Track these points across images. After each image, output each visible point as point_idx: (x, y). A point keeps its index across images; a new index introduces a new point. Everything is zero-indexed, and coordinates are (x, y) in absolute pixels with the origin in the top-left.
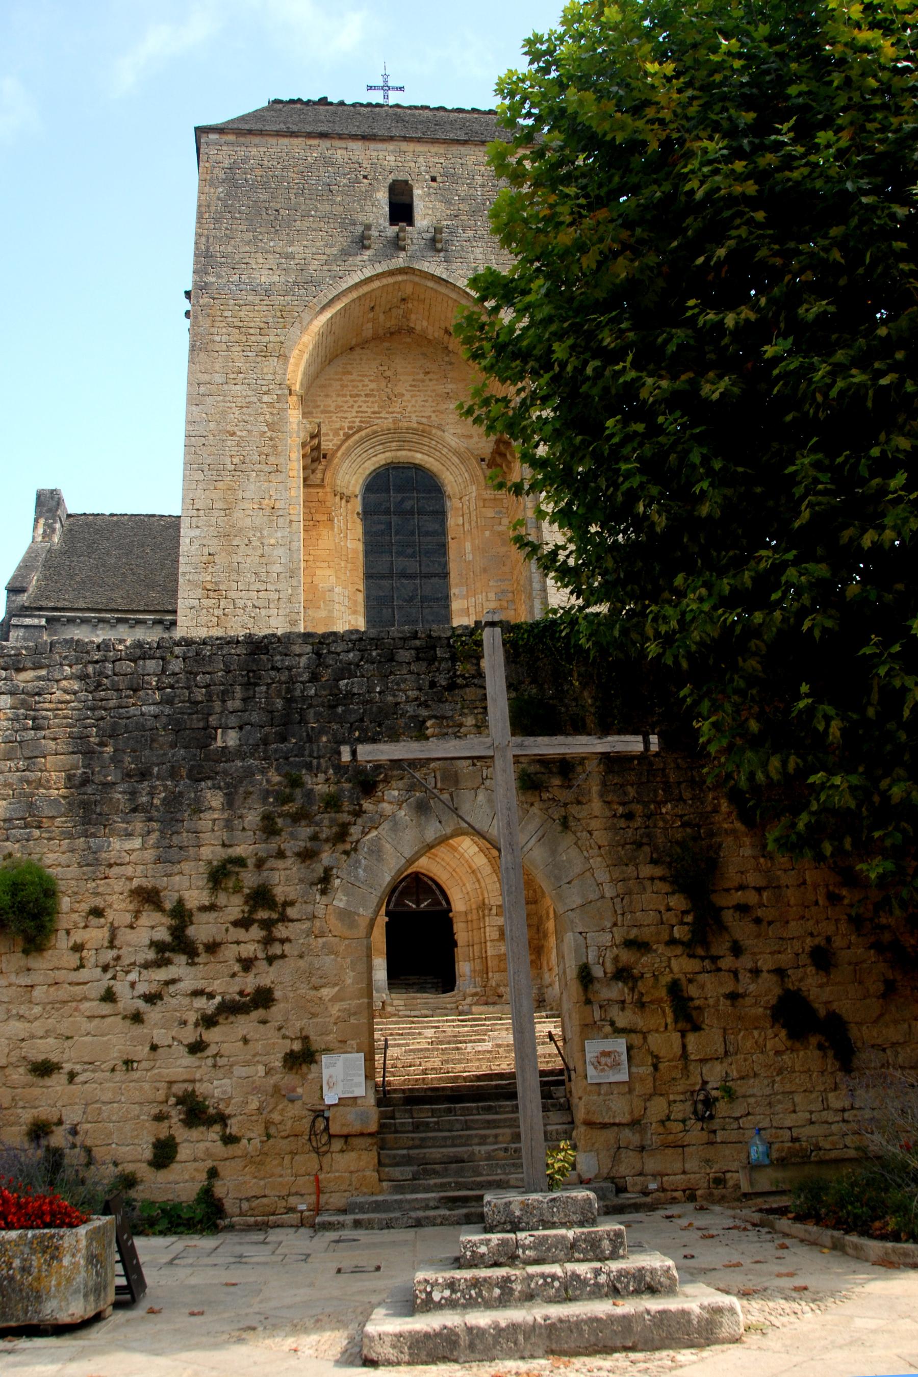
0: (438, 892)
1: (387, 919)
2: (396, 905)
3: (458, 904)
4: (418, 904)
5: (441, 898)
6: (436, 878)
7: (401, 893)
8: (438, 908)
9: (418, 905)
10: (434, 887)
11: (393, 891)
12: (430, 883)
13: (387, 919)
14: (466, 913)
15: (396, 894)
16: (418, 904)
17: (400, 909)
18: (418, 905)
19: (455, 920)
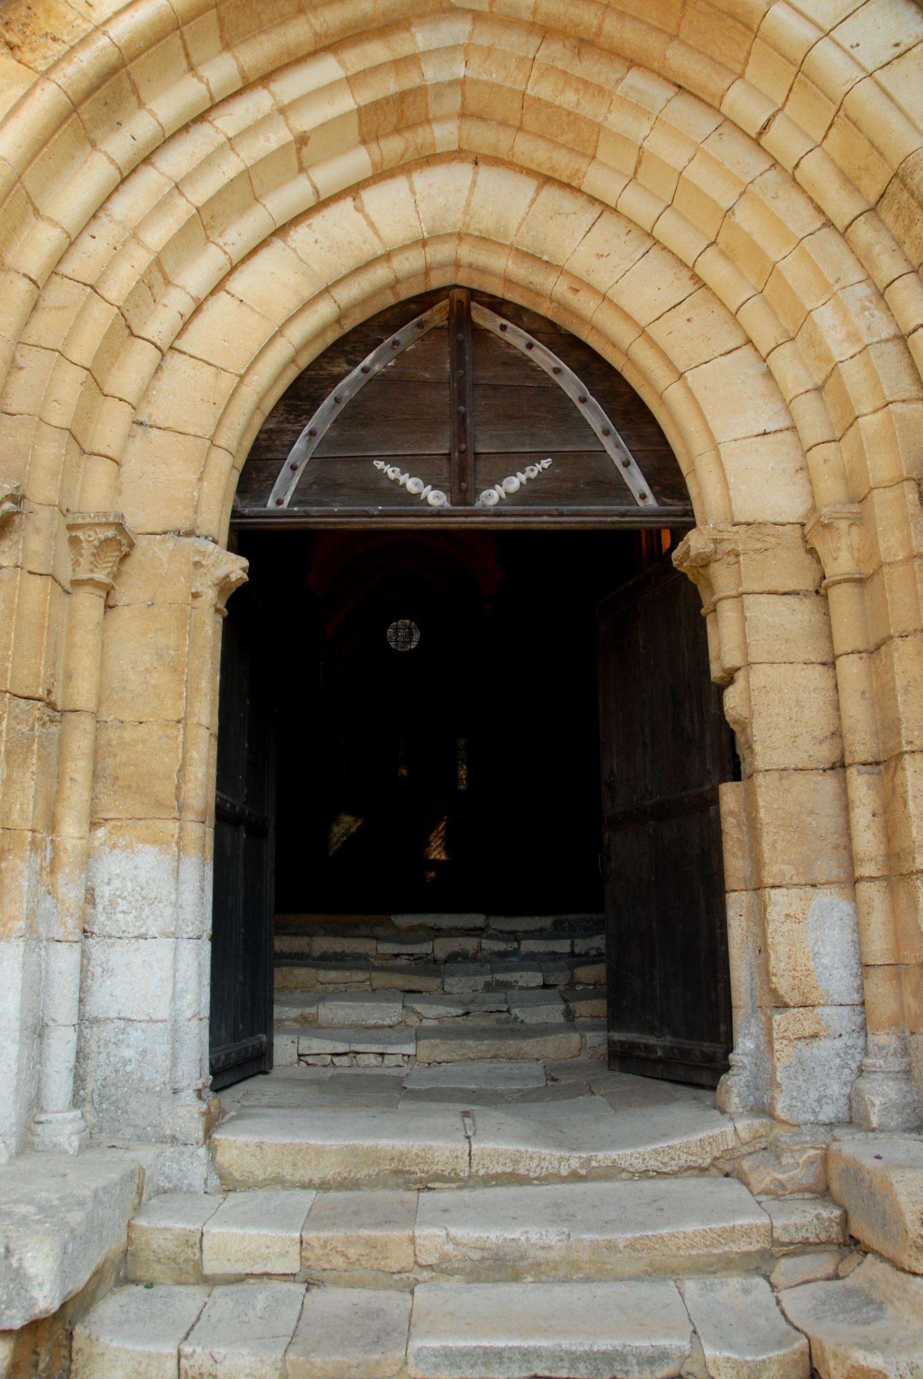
0: (595, 416)
1: (236, 568)
2: (317, 484)
3: (744, 470)
4: (462, 479)
5: (615, 450)
6: (587, 305)
7: (353, 416)
8: (594, 514)
9: (463, 495)
10: (571, 384)
11: (300, 395)
12: (544, 358)
13: (236, 568)
14: (809, 535)
15: (322, 418)
16: (462, 479)
17: (338, 512)
18: (463, 495)
19: (723, 579)
